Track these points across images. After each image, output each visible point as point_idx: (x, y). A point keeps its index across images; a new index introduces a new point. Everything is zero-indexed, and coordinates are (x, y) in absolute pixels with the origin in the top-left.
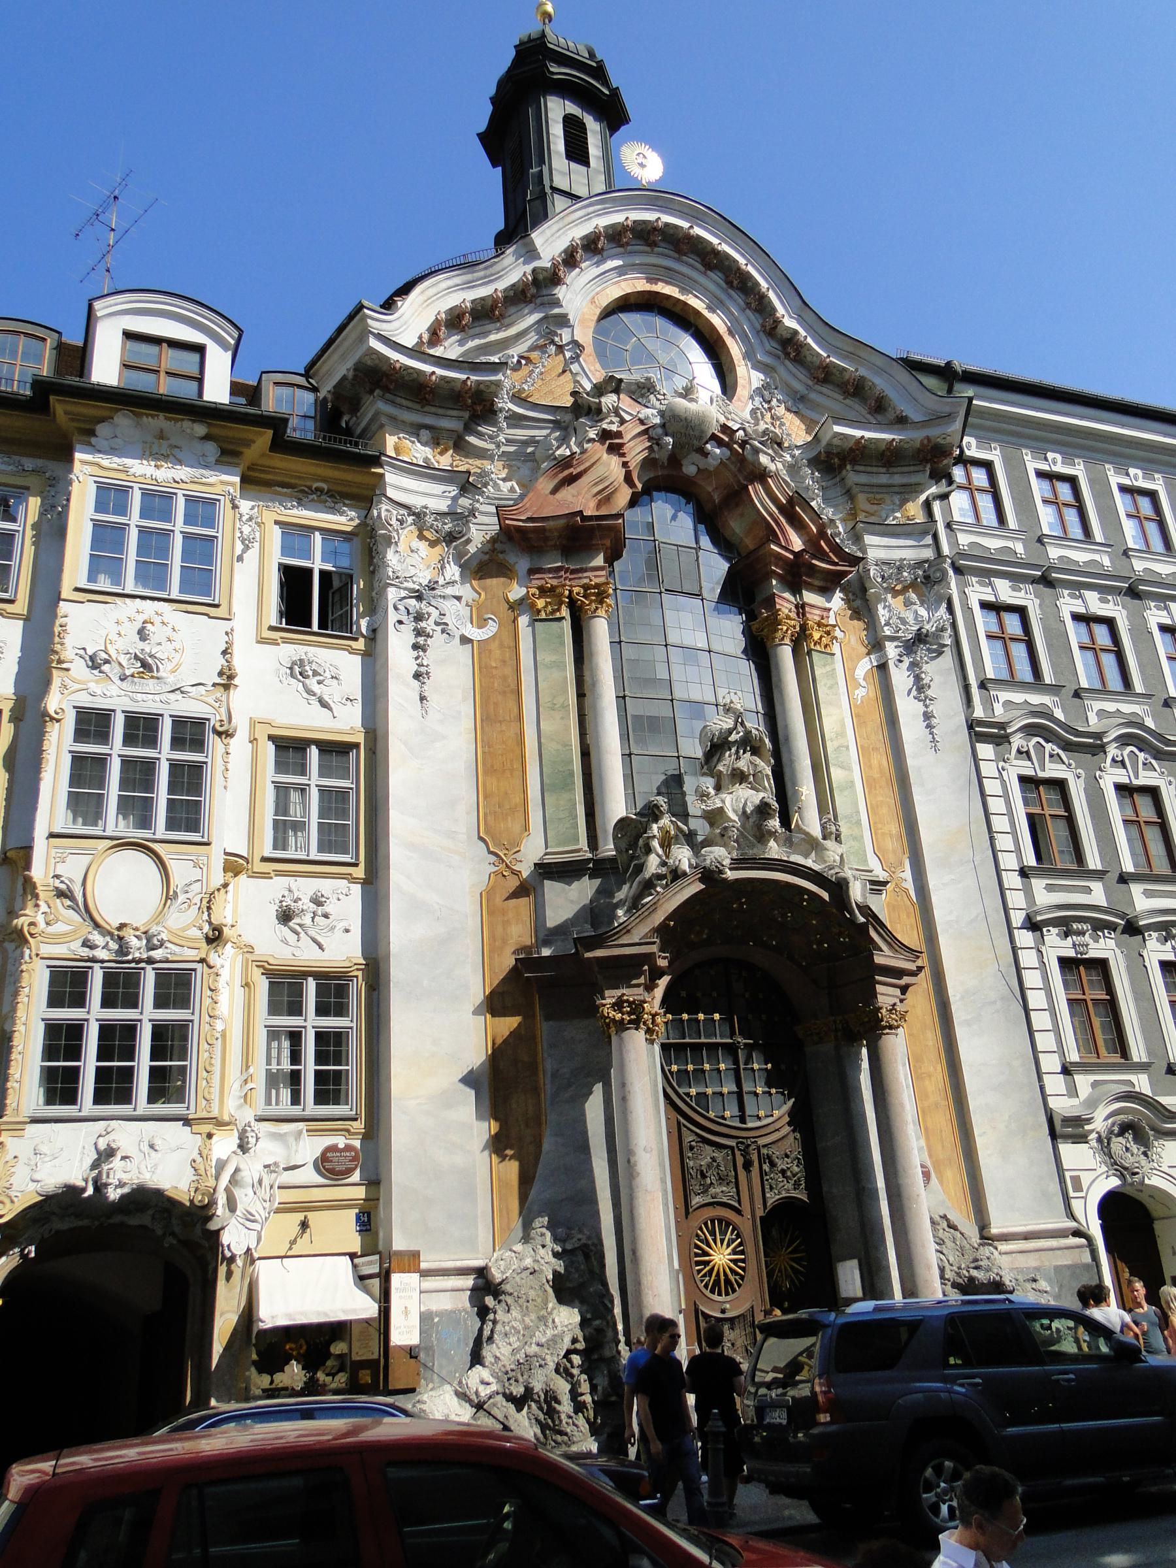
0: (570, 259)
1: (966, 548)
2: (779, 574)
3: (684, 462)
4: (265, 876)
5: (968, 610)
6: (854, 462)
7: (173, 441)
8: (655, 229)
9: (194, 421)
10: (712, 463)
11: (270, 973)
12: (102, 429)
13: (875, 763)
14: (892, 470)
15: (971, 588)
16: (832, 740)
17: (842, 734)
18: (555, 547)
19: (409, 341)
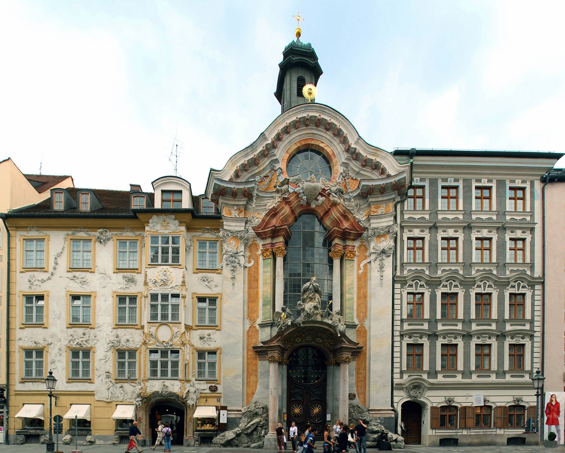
0: (279, 138)
1: (407, 219)
2: (338, 237)
3: (311, 204)
4: (196, 330)
5: (402, 241)
6: (370, 194)
7: (167, 222)
8: (307, 119)
9: (171, 215)
10: (320, 202)
11: (198, 351)
12: (150, 221)
13: (362, 292)
14: (383, 195)
15: (405, 233)
16: (348, 286)
17: (352, 284)
18: (269, 237)
19: (227, 178)
